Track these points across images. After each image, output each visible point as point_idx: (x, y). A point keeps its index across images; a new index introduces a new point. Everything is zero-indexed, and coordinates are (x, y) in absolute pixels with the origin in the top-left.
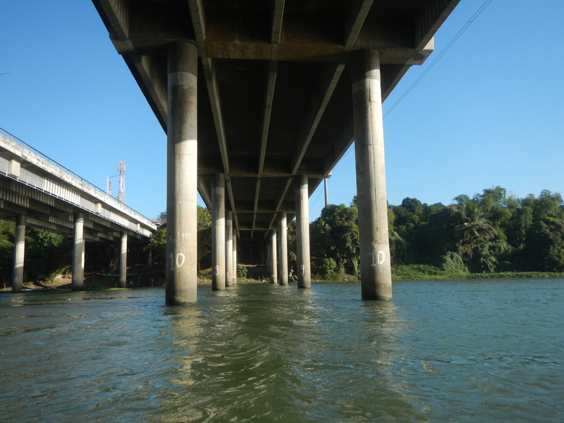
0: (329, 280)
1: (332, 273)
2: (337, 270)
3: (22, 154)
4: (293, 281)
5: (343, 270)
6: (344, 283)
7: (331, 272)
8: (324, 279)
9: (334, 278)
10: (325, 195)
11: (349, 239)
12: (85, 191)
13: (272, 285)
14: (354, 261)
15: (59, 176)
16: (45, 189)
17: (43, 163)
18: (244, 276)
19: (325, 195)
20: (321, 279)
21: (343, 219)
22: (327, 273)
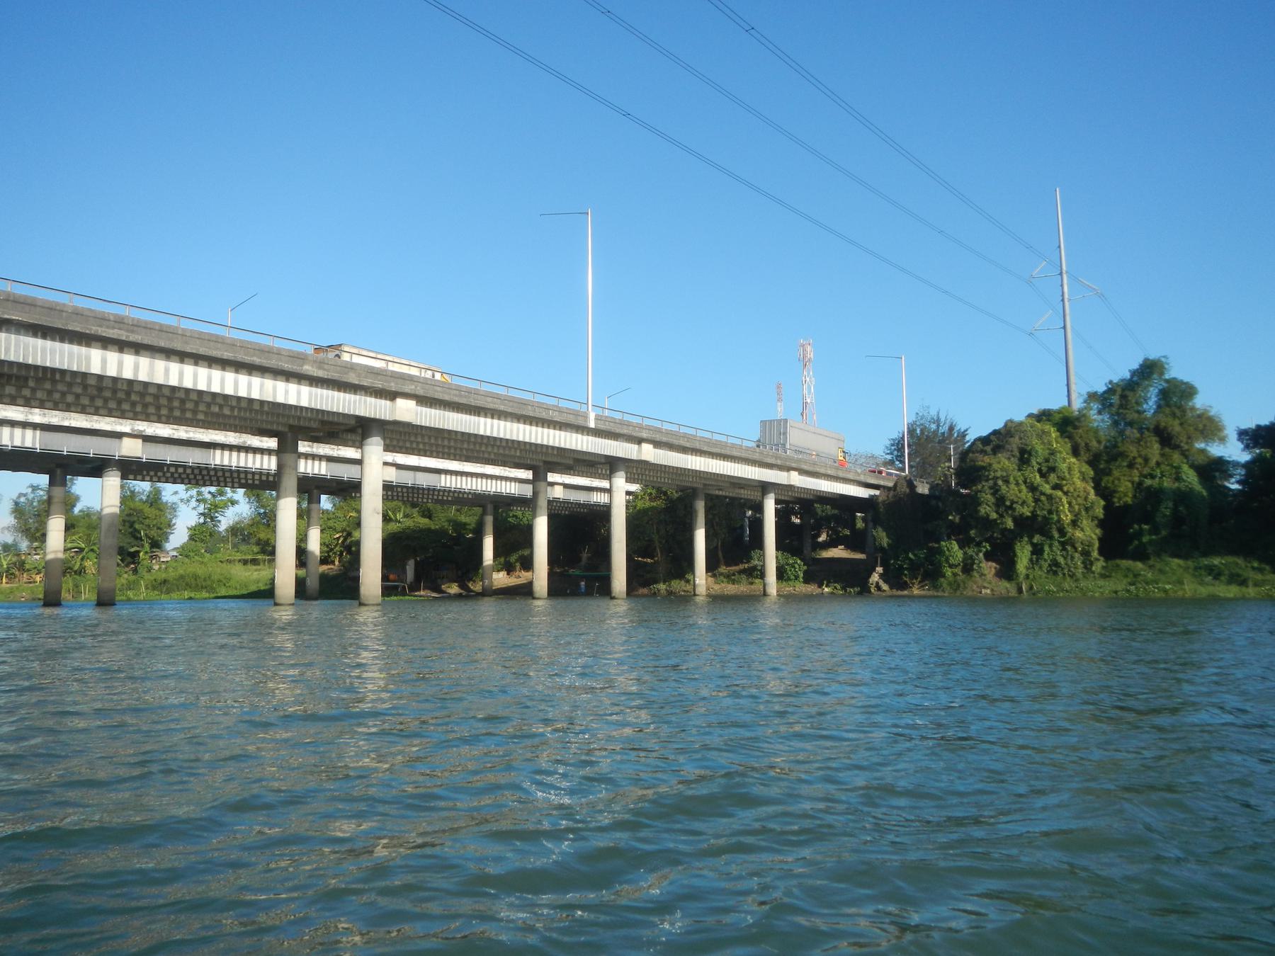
0: (943, 591)
1: (955, 575)
2: (968, 567)
3: (132, 430)
4: (870, 592)
5: (989, 568)
6: (974, 600)
7: (952, 572)
8: (935, 587)
9: (956, 586)
10: (1068, 385)
11: (988, 497)
12: (322, 454)
13: (766, 598)
14: (1018, 547)
15: (234, 443)
16: (218, 462)
17: (187, 432)
18: (797, 578)
19: (1068, 385)
20: (929, 590)
21: (988, 449)
22: (944, 576)
